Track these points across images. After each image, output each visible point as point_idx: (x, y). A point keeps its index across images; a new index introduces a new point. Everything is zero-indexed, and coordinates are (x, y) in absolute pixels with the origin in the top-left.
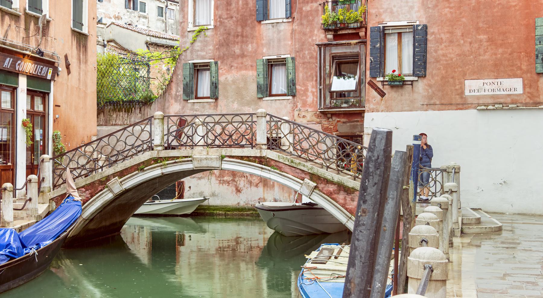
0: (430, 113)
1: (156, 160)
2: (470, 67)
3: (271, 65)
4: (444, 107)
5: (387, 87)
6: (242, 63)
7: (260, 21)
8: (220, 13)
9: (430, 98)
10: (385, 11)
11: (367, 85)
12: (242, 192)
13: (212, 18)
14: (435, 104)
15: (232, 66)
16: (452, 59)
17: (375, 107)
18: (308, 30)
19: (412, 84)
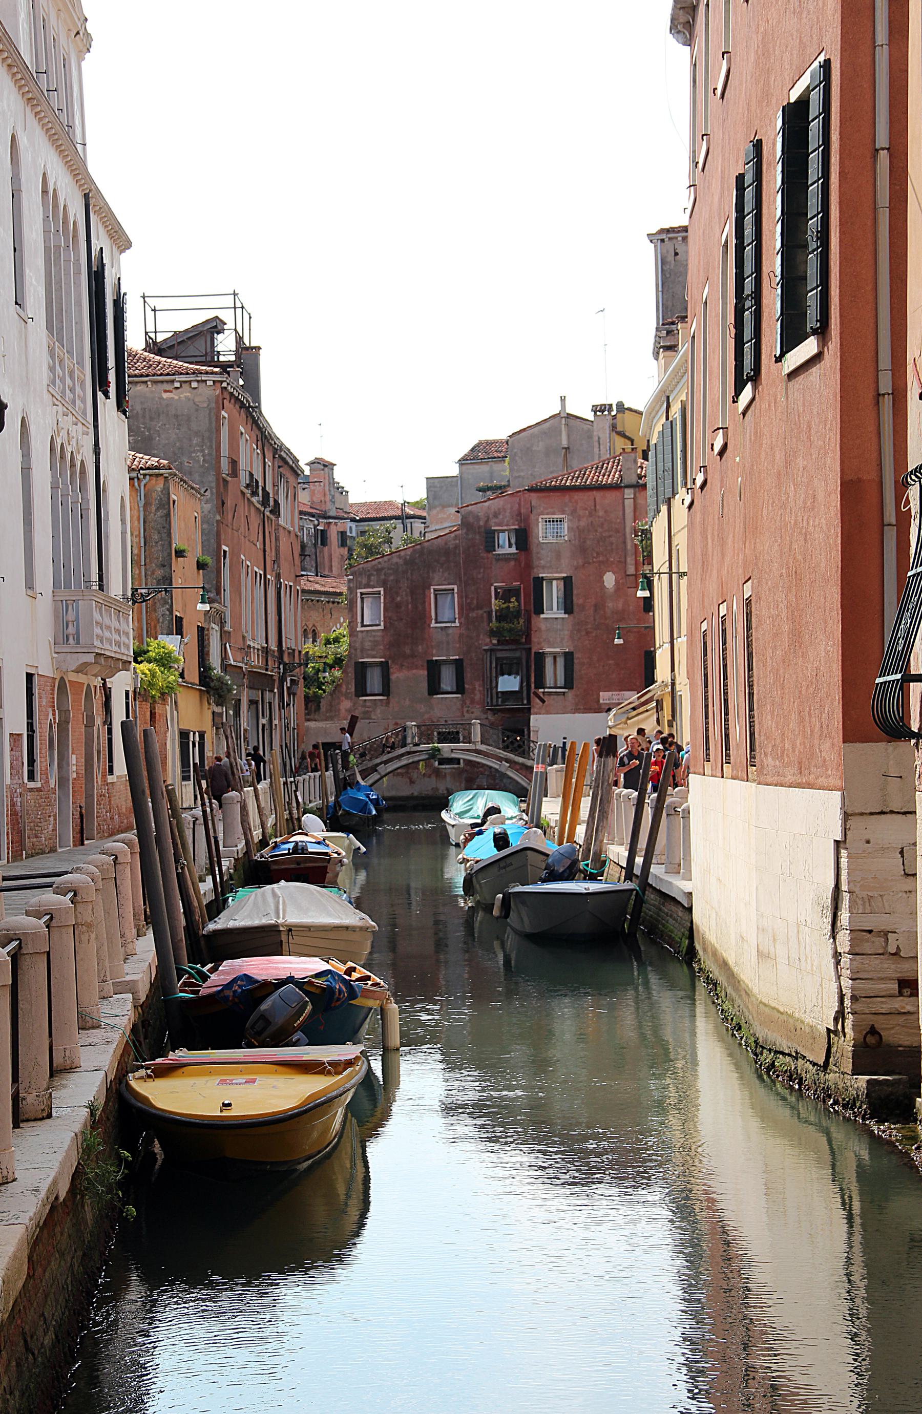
0: (577, 715)
1: (409, 753)
8: (390, 614)
9: (577, 704)
10: (544, 640)
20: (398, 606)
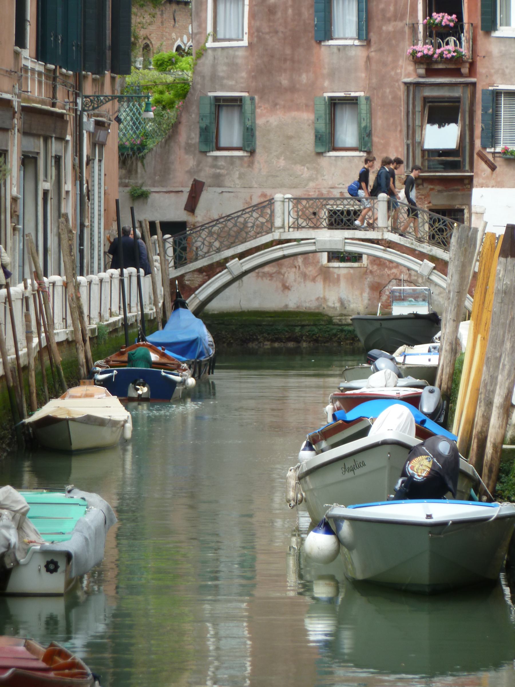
3: (334, 104)
5: (498, 159)
6: (292, 101)
7: (320, 42)
8: (258, 24)
11: (475, 156)
12: (293, 289)
13: (246, 30)
15: (276, 105)
17: (484, 181)
18: (390, 59)
20: (272, 11)
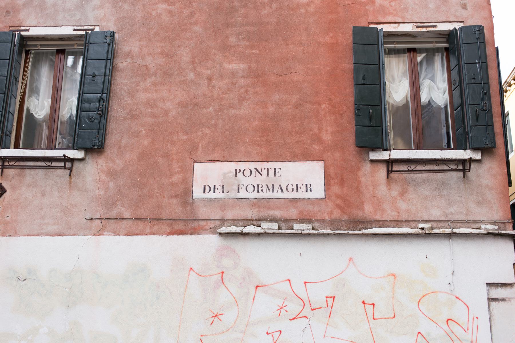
0: (108, 241)
2: (207, 131)
4: (140, 226)
9: (110, 203)
14: (120, 219)
16: (166, 113)
19: (71, 169)
